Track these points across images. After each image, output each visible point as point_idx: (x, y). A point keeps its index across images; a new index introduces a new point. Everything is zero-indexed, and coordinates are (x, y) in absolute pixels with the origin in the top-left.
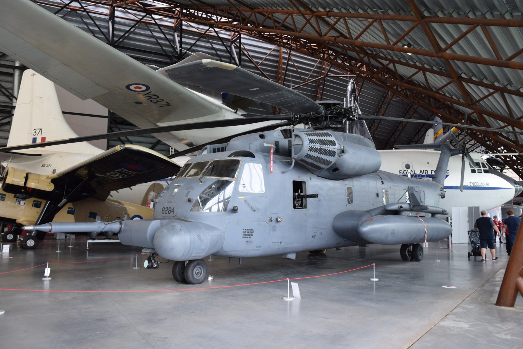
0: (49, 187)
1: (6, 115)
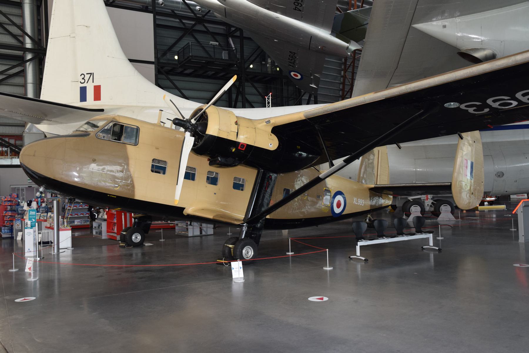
0: (271, 143)
1: (14, 63)
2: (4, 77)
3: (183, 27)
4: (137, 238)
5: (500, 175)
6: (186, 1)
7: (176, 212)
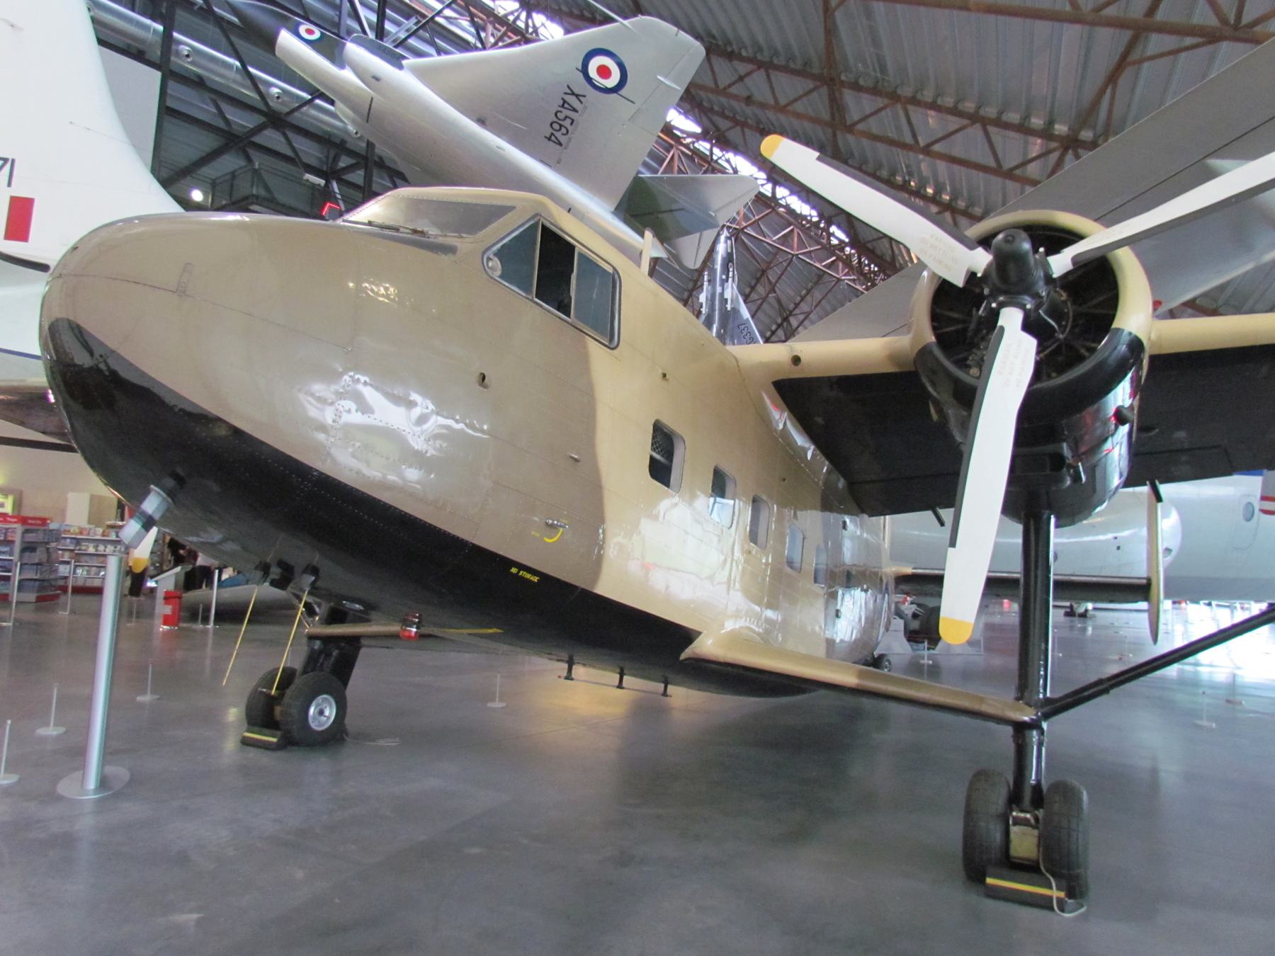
6: (251, 69)
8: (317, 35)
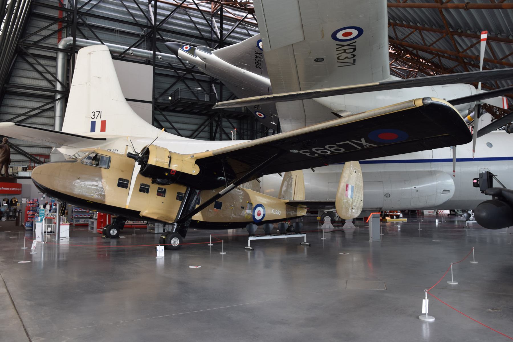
0: (194, 170)
1: (48, 101)
2: (40, 111)
3: (177, 75)
4: (114, 232)
5: (388, 196)
7: (134, 214)
8: (189, 48)
